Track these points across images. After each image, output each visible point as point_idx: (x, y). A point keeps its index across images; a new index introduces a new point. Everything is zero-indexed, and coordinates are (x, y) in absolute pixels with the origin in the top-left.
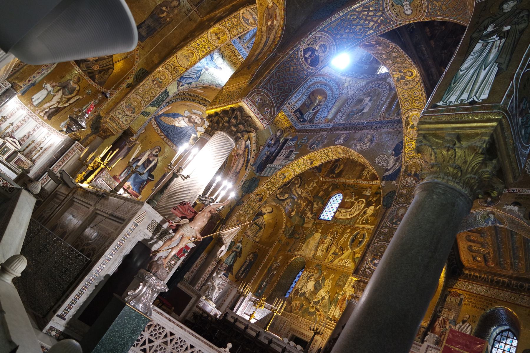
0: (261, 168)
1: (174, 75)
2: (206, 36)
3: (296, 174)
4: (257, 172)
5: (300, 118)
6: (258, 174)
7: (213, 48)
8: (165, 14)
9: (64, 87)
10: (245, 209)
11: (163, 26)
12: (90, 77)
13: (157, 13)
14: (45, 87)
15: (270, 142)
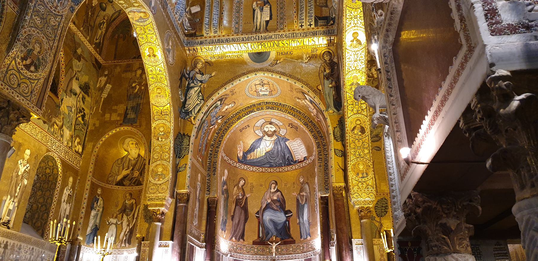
0: (338, 103)
1: (166, 119)
2: (147, 66)
3: (364, 70)
4: (338, 111)
5: (328, 23)
6: (341, 112)
7: (163, 67)
8: (138, 87)
9: (124, 210)
10: (355, 155)
11: (143, 95)
12: (137, 185)
13: (131, 93)
14: (109, 223)
15: (325, 73)
